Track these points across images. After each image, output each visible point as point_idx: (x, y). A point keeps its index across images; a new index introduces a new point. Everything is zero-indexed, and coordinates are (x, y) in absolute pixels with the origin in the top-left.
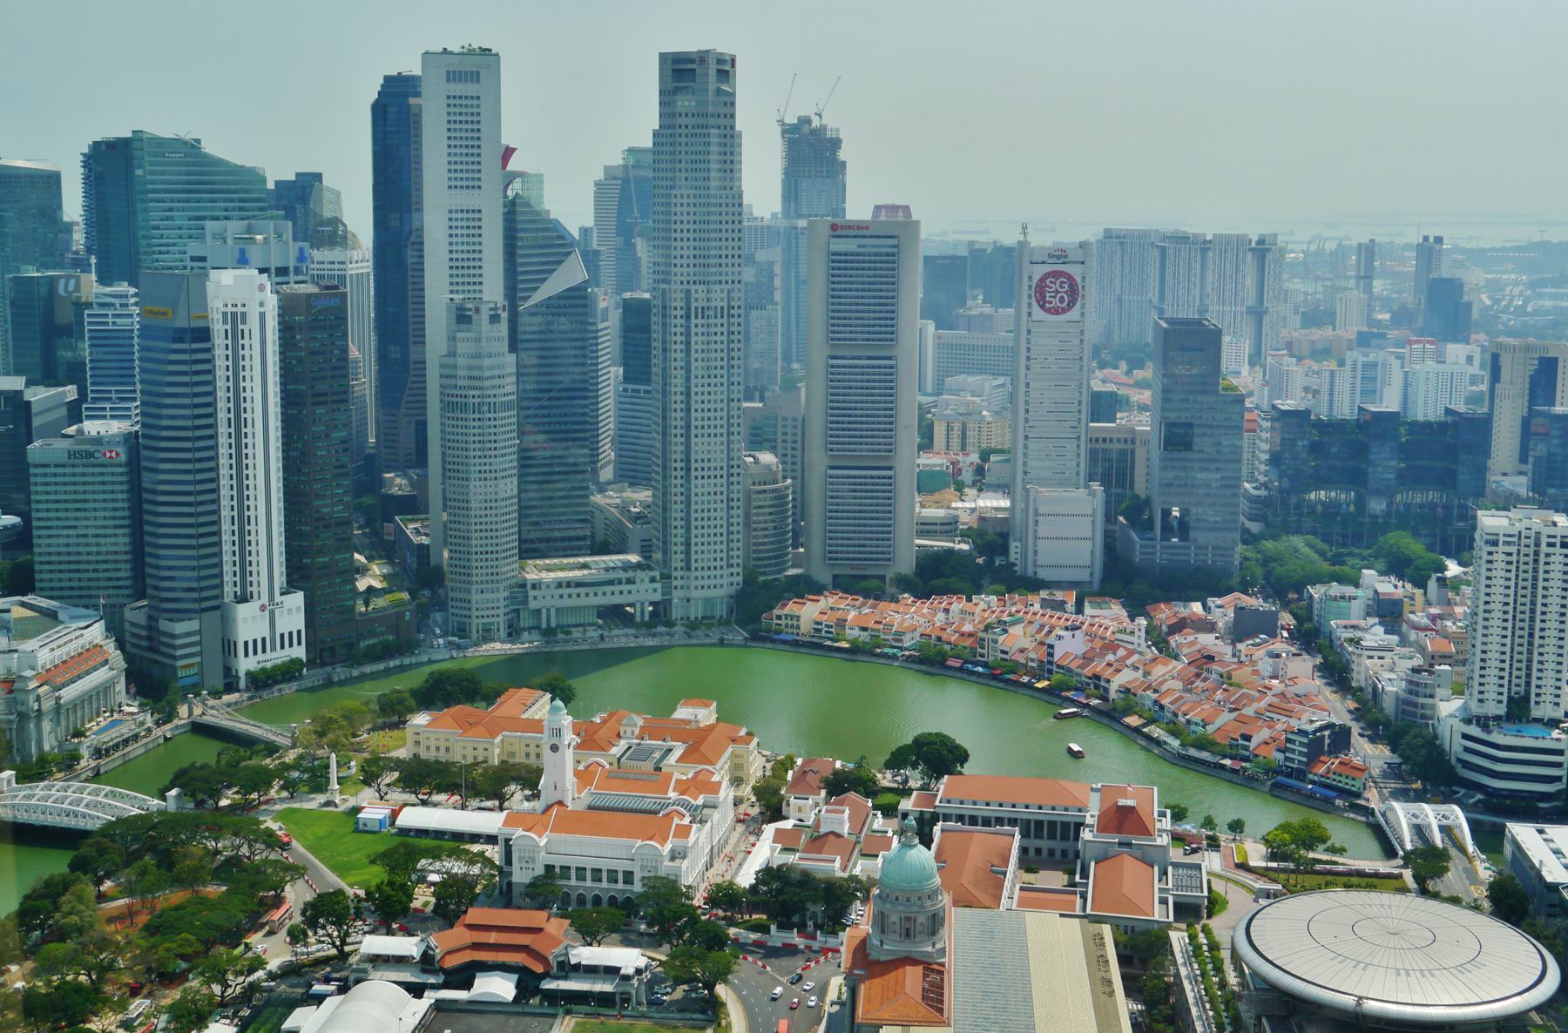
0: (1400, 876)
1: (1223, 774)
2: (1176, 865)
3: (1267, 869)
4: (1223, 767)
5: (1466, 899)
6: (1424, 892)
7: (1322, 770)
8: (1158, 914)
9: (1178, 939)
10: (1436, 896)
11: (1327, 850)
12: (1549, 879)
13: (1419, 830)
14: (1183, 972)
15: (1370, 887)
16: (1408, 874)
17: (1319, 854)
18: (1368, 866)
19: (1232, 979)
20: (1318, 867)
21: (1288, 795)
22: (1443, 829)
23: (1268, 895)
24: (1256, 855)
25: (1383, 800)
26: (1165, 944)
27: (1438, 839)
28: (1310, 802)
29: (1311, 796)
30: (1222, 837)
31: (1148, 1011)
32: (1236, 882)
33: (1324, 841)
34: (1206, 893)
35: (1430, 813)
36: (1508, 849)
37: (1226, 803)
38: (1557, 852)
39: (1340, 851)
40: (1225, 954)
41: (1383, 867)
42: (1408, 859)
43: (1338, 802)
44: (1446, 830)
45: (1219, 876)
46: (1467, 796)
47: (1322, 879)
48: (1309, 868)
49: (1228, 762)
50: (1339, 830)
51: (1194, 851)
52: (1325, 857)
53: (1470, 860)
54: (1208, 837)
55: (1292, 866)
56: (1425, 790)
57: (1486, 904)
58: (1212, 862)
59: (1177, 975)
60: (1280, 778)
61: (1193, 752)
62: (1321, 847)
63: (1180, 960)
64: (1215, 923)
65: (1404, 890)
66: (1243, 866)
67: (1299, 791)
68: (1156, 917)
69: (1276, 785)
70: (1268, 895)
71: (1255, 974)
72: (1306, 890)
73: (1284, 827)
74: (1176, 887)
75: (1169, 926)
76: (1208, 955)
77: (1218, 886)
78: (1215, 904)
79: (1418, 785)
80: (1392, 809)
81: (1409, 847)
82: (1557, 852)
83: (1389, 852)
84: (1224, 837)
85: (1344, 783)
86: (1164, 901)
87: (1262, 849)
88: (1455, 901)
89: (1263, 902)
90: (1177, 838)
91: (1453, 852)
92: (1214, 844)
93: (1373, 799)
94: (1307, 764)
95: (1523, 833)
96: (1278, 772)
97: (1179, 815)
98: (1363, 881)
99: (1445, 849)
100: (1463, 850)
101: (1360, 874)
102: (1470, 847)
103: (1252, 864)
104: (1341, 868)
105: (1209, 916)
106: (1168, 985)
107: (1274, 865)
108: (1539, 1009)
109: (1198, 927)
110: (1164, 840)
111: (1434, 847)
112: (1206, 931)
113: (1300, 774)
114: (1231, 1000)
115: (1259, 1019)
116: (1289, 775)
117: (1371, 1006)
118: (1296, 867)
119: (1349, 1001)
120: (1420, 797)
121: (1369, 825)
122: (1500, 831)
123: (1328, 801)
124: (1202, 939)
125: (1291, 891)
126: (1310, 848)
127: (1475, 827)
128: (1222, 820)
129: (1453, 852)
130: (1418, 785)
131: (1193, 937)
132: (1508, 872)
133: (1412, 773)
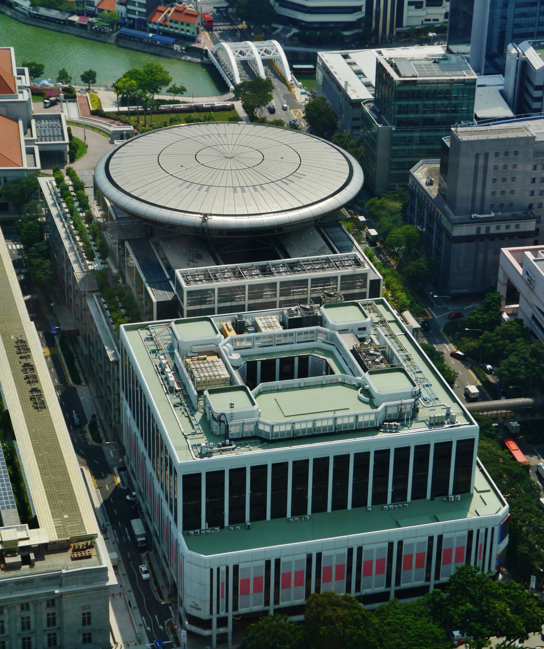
0: (232, 108)
1: (72, 30)
2: (38, 118)
3: (119, 113)
4: (72, 23)
5: (287, 121)
6: (253, 119)
7: (160, 19)
8: (26, 164)
9: (46, 183)
10: (262, 122)
11: (169, 91)
12: (353, 97)
13: (246, 66)
14: (54, 211)
15: (208, 120)
16: (238, 105)
17: (162, 96)
18: (204, 101)
19: (97, 212)
20: (163, 107)
21: (132, 44)
22: (265, 62)
23: (121, 136)
24: (109, 101)
25: (216, 42)
26: (37, 191)
27: (262, 72)
28: (152, 50)
29: (152, 43)
30: (77, 88)
31: (26, 249)
32: (93, 128)
33: (166, 82)
34: (67, 140)
35: (254, 49)
36: (320, 75)
37: (78, 57)
38: (359, 73)
39: (180, 91)
40: (89, 192)
41: (218, 101)
42: (239, 91)
43: (176, 47)
44: (268, 63)
45: (78, 124)
46: (285, 31)
47: (166, 118)
48: (155, 108)
49: (75, 18)
50: (178, 72)
51: (53, 104)
52: (168, 98)
53: (289, 87)
54: (65, 90)
55: (140, 108)
56: (249, 30)
57: (303, 124)
58: (70, 111)
59: (49, 215)
60: (124, 29)
61: (43, 11)
62: (164, 89)
63: (50, 201)
64: (78, 166)
65: (236, 119)
66: (98, 113)
67: (141, 40)
68: (25, 167)
69: (120, 37)
70: (121, 136)
71: (116, 206)
72: (154, 128)
73: (130, 75)
74: (40, 138)
75: (37, 173)
76: (73, 195)
77: (78, 133)
78: (76, 149)
79: (243, 25)
80: (223, 49)
81: (238, 81)
82: (359, 73)
83: (222, 87)
84: (78, 87)
85: (179, 29)
86: (30, 152)
87: (114, 96)
88: (278, 124)
89: (118, 143)
90: (37, 93)
91: (275, 82)
92: (70, 95)
93: (205, 41)
94: (146, 14)
95: (331, 59)
96: (122, 24)
97: (36, 72)
98: (202, 115)
99: (269, 81)
100: (283, 79)
101: (199, 109)
102: (289, 76)
103: (106, 109)
104: (182, 106)
105: (72, 160)
106: (42, 224)
107: (125, 109)
108: (349, 205)
109: (63, 171)
110: (25, 96)
111: (259, 79)
112: (71, 173)
113: (141, 25)
114: (97, 231)
115: (122, 243)
116: (132, 26)
117: (214, 220)
118: (144, 108)
119: (197, 219)
120: (244, 36)
121: (203, 65)
122: (313, 59)
123: (167, 47)
124: (68, 181)
125: (142, 130)
126: (155, 90)
127: (292, 58)
128: (76, 73)
129: (275, 82)
130: (243, 25)
131: (59, 181)
132: (320, 94)
133: (238, 15)
